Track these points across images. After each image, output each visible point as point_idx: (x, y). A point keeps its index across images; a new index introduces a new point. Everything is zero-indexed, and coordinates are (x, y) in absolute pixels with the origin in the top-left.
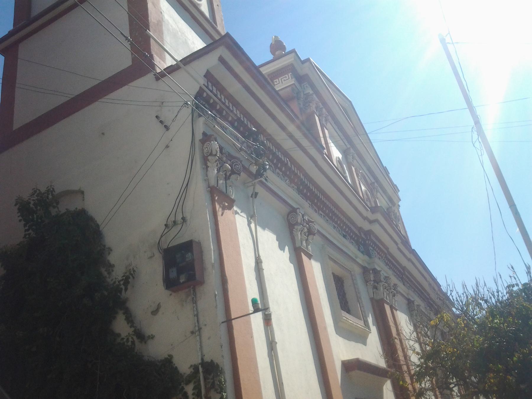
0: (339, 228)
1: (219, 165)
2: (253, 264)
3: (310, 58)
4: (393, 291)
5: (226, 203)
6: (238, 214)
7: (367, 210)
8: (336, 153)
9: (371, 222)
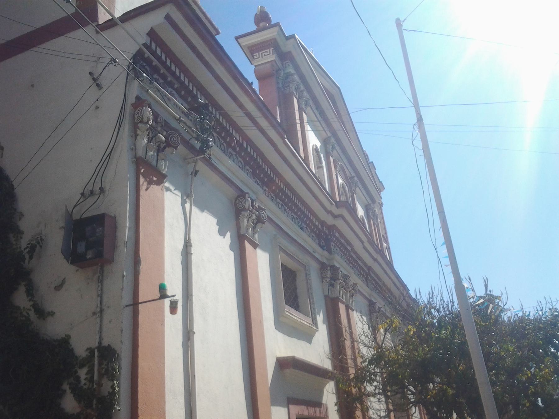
1: (151, 135)
2: (180, 246)
3: (295, 35)
4: (352, 291)
6: (170, 190)
7: (332, 204)
8: (313, 141)
9: (335, 217)
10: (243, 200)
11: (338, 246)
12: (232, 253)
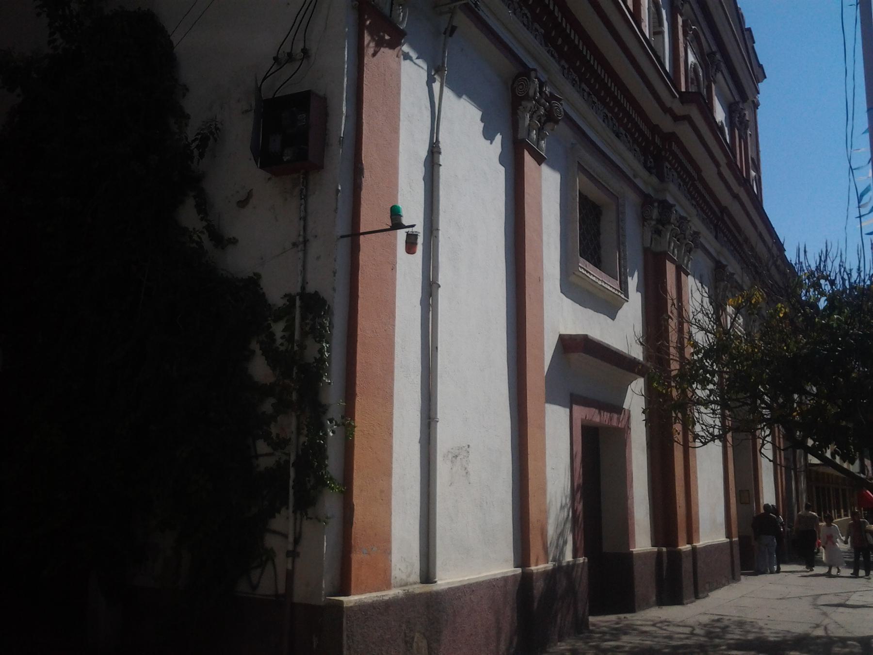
0: (614, 119)
2: (423, 152)
5: (386, 35)
6: (411, 59)
9: (676, 118)
10: (526, 80)
11: (676, 170)
12: (502, 169)
